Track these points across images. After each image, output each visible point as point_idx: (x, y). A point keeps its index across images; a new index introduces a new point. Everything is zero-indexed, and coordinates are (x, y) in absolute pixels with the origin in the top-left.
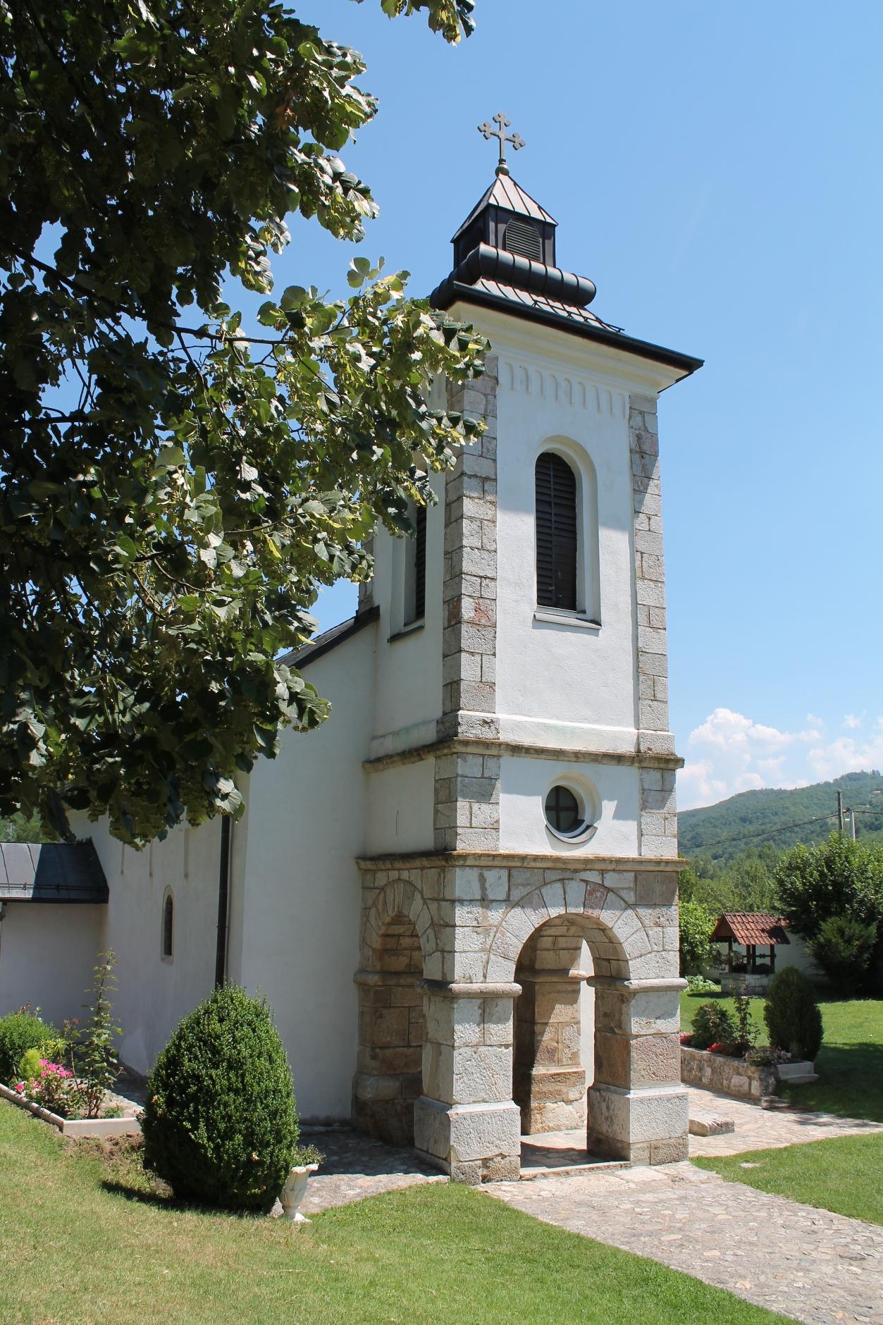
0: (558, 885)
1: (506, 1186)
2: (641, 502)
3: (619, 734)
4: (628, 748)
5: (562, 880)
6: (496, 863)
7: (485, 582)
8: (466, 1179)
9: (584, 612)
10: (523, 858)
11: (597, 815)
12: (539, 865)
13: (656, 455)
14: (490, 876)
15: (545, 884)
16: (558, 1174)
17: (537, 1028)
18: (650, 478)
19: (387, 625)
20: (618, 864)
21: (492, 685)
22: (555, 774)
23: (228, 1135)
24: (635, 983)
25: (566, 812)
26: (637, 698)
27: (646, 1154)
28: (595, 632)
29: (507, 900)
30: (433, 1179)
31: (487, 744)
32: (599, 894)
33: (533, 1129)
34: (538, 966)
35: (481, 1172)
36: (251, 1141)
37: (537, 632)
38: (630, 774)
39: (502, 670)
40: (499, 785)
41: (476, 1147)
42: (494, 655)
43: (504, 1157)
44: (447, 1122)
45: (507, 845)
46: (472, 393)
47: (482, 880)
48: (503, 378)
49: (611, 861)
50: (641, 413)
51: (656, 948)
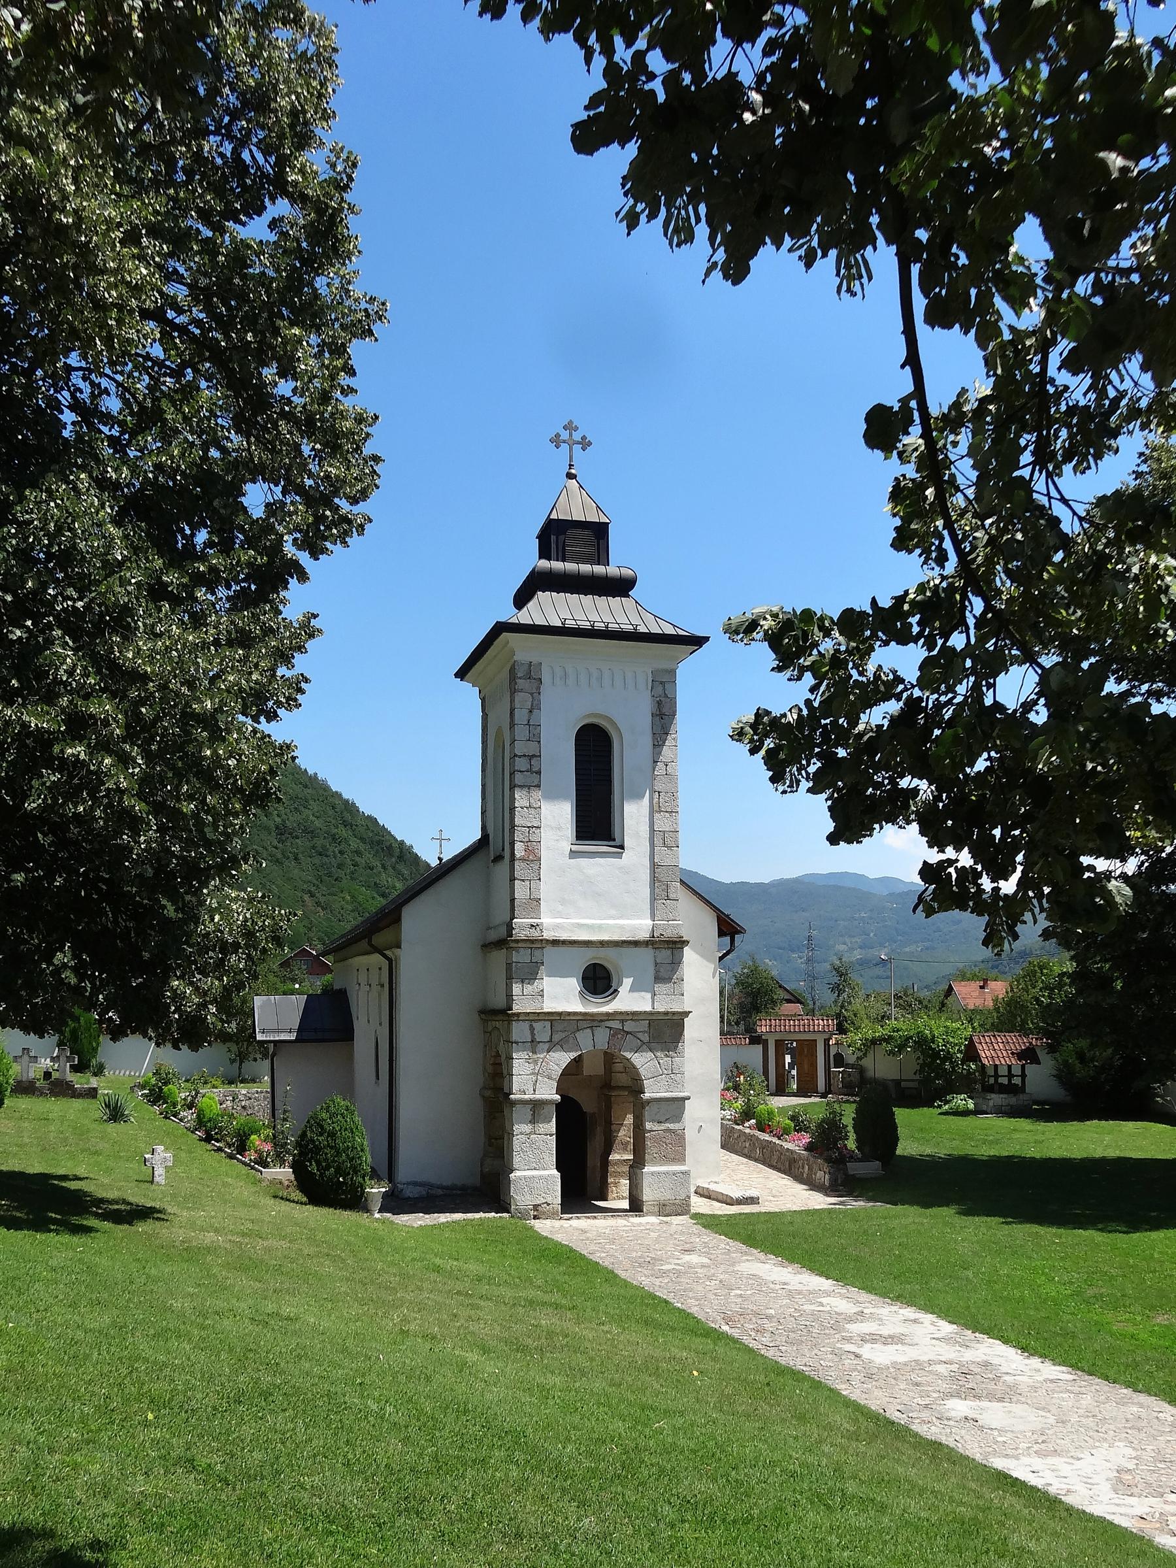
0: (589, 1030)
1: (548, 1222)
3: (640, 925)
4: (644, 935)
8: (524, 1216)
10: (560, 1014)
11: (620, 983)
17: (613, 1127)
20: (634, 1016)
23: (328, 1168)
24: (647, 1095)
25: (598, 981)
26: (653, 899)
27: (656, 1209)
28: (619, 856)
31: (532, 941)
33: (610, 1197)
36: (339, 1171)
38: (647, 954)
39: (547, 889)
47: (532, 1029)
48: (546, 678)
49: (627, 1013)
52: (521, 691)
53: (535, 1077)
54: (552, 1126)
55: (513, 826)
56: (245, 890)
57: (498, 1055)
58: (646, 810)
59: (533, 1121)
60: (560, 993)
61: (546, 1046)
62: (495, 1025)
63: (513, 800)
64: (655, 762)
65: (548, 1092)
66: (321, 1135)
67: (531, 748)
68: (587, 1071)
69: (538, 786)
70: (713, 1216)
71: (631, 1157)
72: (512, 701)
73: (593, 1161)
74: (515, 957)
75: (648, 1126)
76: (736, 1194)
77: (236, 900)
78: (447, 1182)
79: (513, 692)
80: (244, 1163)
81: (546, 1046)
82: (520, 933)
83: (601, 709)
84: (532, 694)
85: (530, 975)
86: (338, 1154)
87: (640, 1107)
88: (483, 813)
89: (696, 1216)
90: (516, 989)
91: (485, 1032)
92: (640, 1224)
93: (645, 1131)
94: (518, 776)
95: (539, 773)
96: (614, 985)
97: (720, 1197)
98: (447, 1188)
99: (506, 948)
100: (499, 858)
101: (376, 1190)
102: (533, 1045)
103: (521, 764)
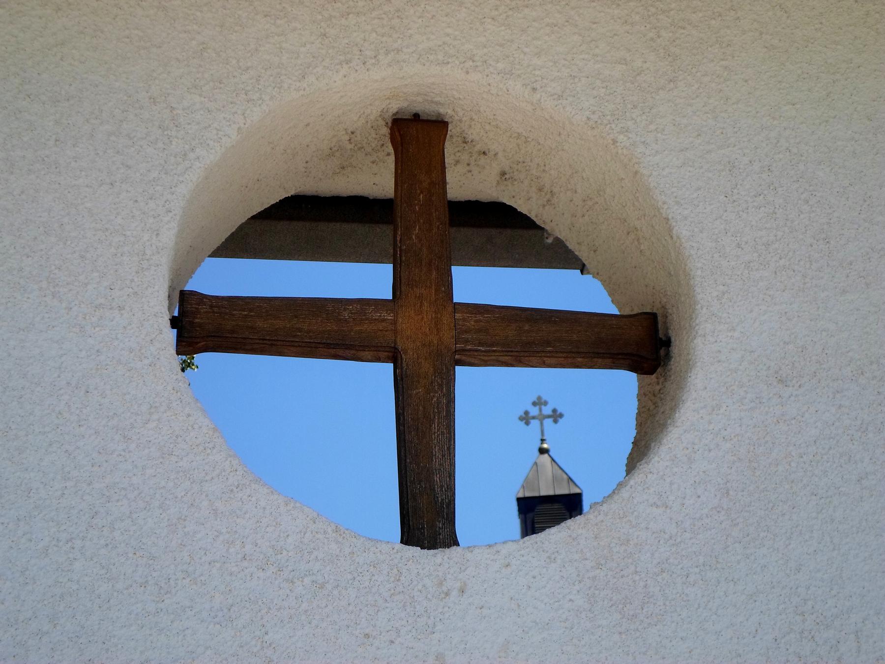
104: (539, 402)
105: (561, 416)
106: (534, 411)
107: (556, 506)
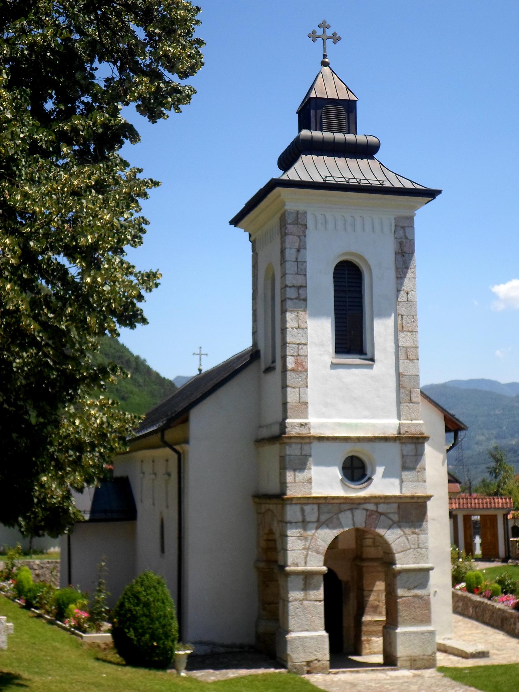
0: (349, 513)
2: (402, 284)
3: (388, 424)
4: (392, 432)
5: (351, 509)
6: (310, 501)
7: (300, 346)
8: (298, 671)
9: (366, 354)
10: (326, 498)
11: (373, 472)
12: (336, 501)
13: (412, 252)
14: (307, 508)
15: (340, 512)
16: (352, 672)
17: (366, 593)
18: (407, 268)
19: (263, 362)
20: (386, 500)
21: (306, 404)
22: (348, 450)
23: (143, 634)
24: (398, 566)
25: (355, 470)
26: (399, 403)
27: (408, 664)
28: (371, 367)
29: (318, 521)
30: (278, 671)
31: (302, 438)
32: (375, 517)
33: (364, 652)
34: (364, 556)
35: (306, 668)
36: (154, 637)
37: (334, 372)
38: (395, 449)
39: (312, 394)
40: (311, 459)
41: (302, 655)
42: (307, 387)
43: (319, 661)
44: (285, 642)
45: (317, 491)
46: (291, 237)
47: (303, 511)
48: (310, 223)
49: (380, 498)
50: (403, 227)
51: (413, 546)
52: (291, 234)
53: (306, 551)
54: (320, 593)
55: (284, 344)
56: (97, 398)
57: (271, 532)
58: (392, 330)
59: (306, 588)
60: (324, 481)
61: (315, 525)
62: (269, 510)
63: (284, 321)
64: (398, 291)
65: (317, 564)
66: (138, 605)
67: (298, 280)
68: (341, 546)
69: (305, 311)
70: (456, 669)
71: (384, 618)
72: (283, 242)
73: (348, 621)
74: (289, 451)
75: (400, 592)
76: (470, 649)
77: (91, 406)
78: (227, 641)
79: (283, 235)
80: (65, 629)
81: (315, 525)
82: (291, 431)
83: (354, 249)
84: (299, 237)
85: (301, 465)
86: (152, 620)
87: (392, 577)
88: (254, 333)
89: (442, 669)
90: (290, 476)
91: (259, 513)
92: (397, 678)
93: (396, 597)
94: (289, 303)
95: (305, 300)
96: (369, 473)
97: (456, 652)
98: (228, 646)
99: (278, 442)
100: (269, 369)
101: (182, 652)
102: (304, 524)
103: (291, 293)
104: (323, 26)
105: (339, 39)
106: (320, 32)
107: (338, 107)
